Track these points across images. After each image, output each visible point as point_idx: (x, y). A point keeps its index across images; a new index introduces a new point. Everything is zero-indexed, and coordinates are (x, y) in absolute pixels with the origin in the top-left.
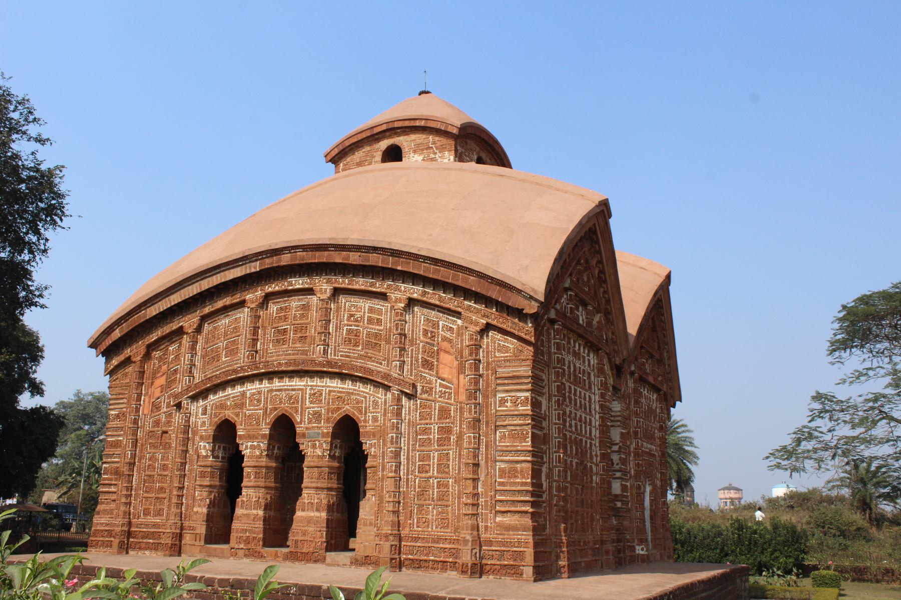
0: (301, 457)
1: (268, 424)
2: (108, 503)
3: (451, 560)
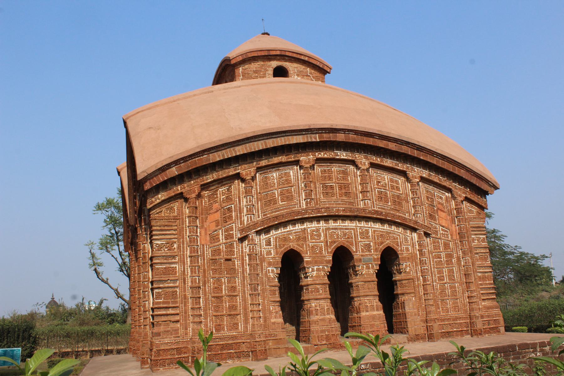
1: (331, 252)
3: (465, 329)
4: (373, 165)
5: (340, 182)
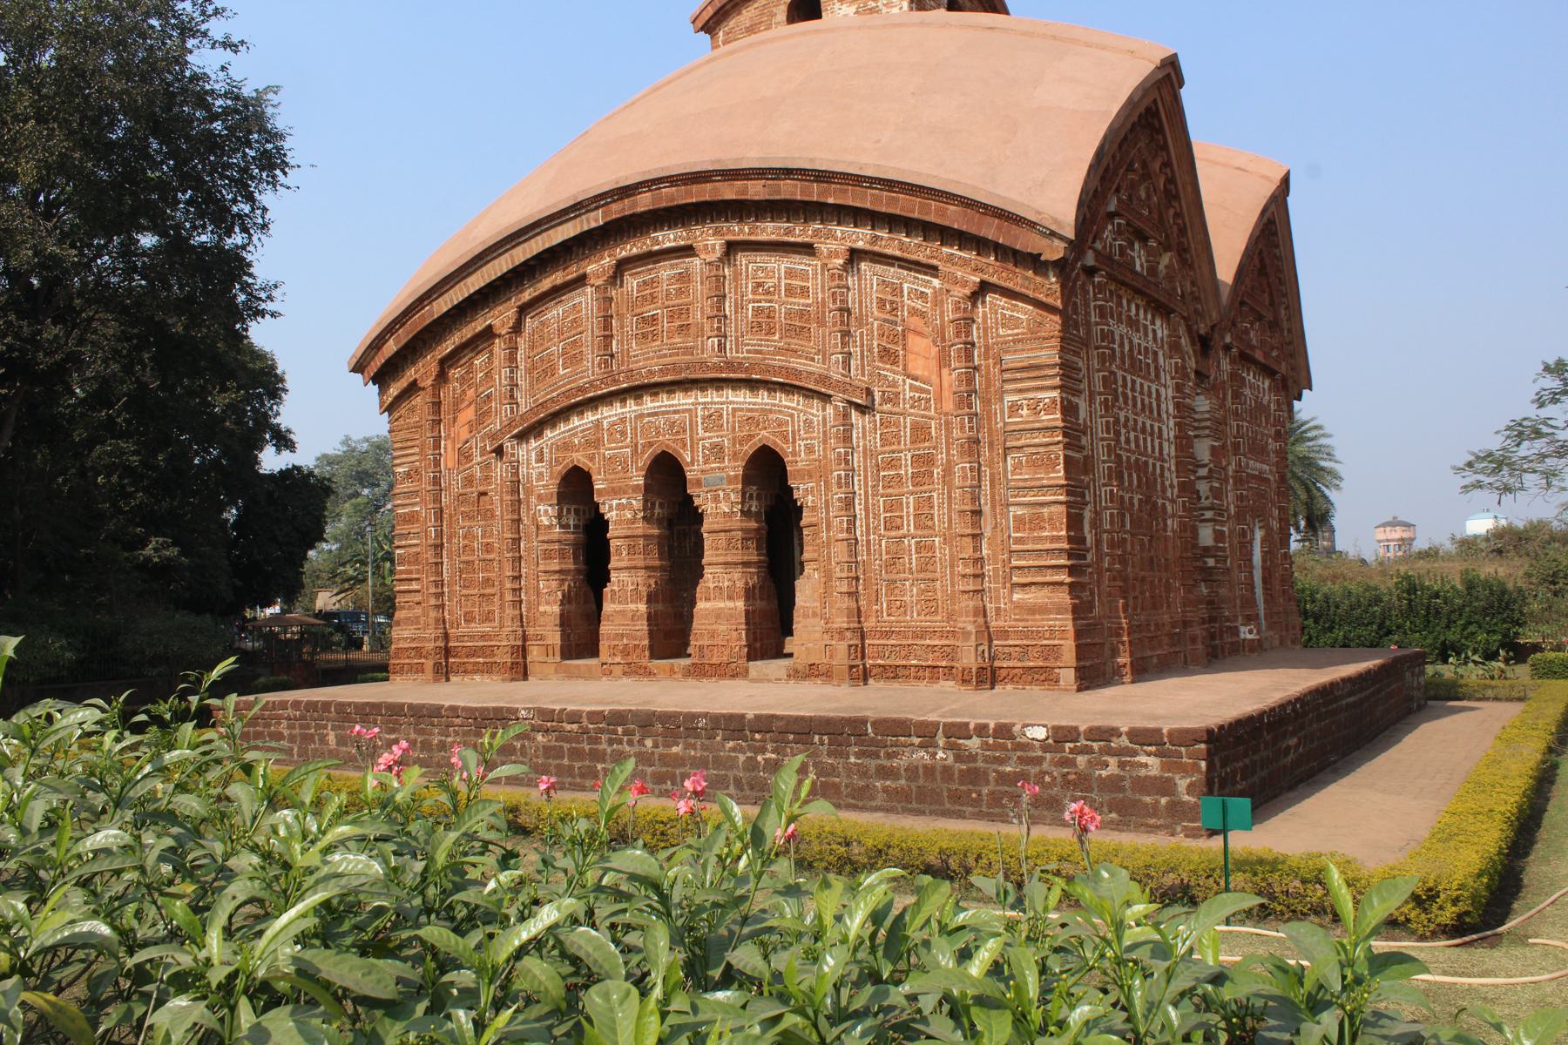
0: (698, 518)
2: (410, 608)
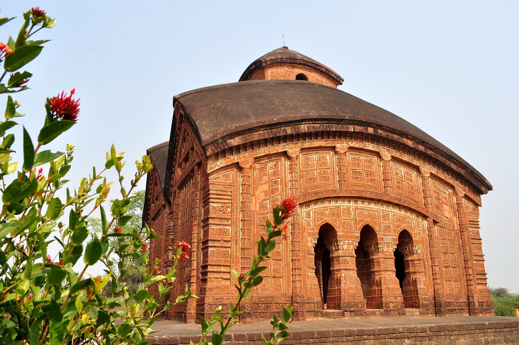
4: (394, 159)
5: (367, 169)
